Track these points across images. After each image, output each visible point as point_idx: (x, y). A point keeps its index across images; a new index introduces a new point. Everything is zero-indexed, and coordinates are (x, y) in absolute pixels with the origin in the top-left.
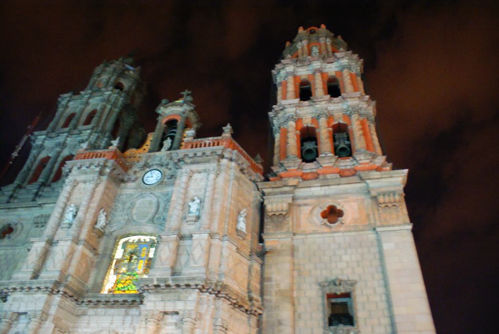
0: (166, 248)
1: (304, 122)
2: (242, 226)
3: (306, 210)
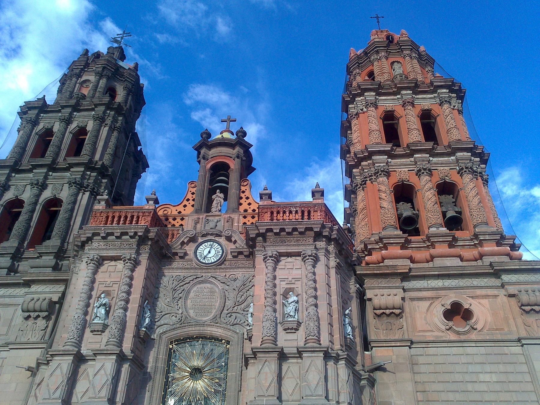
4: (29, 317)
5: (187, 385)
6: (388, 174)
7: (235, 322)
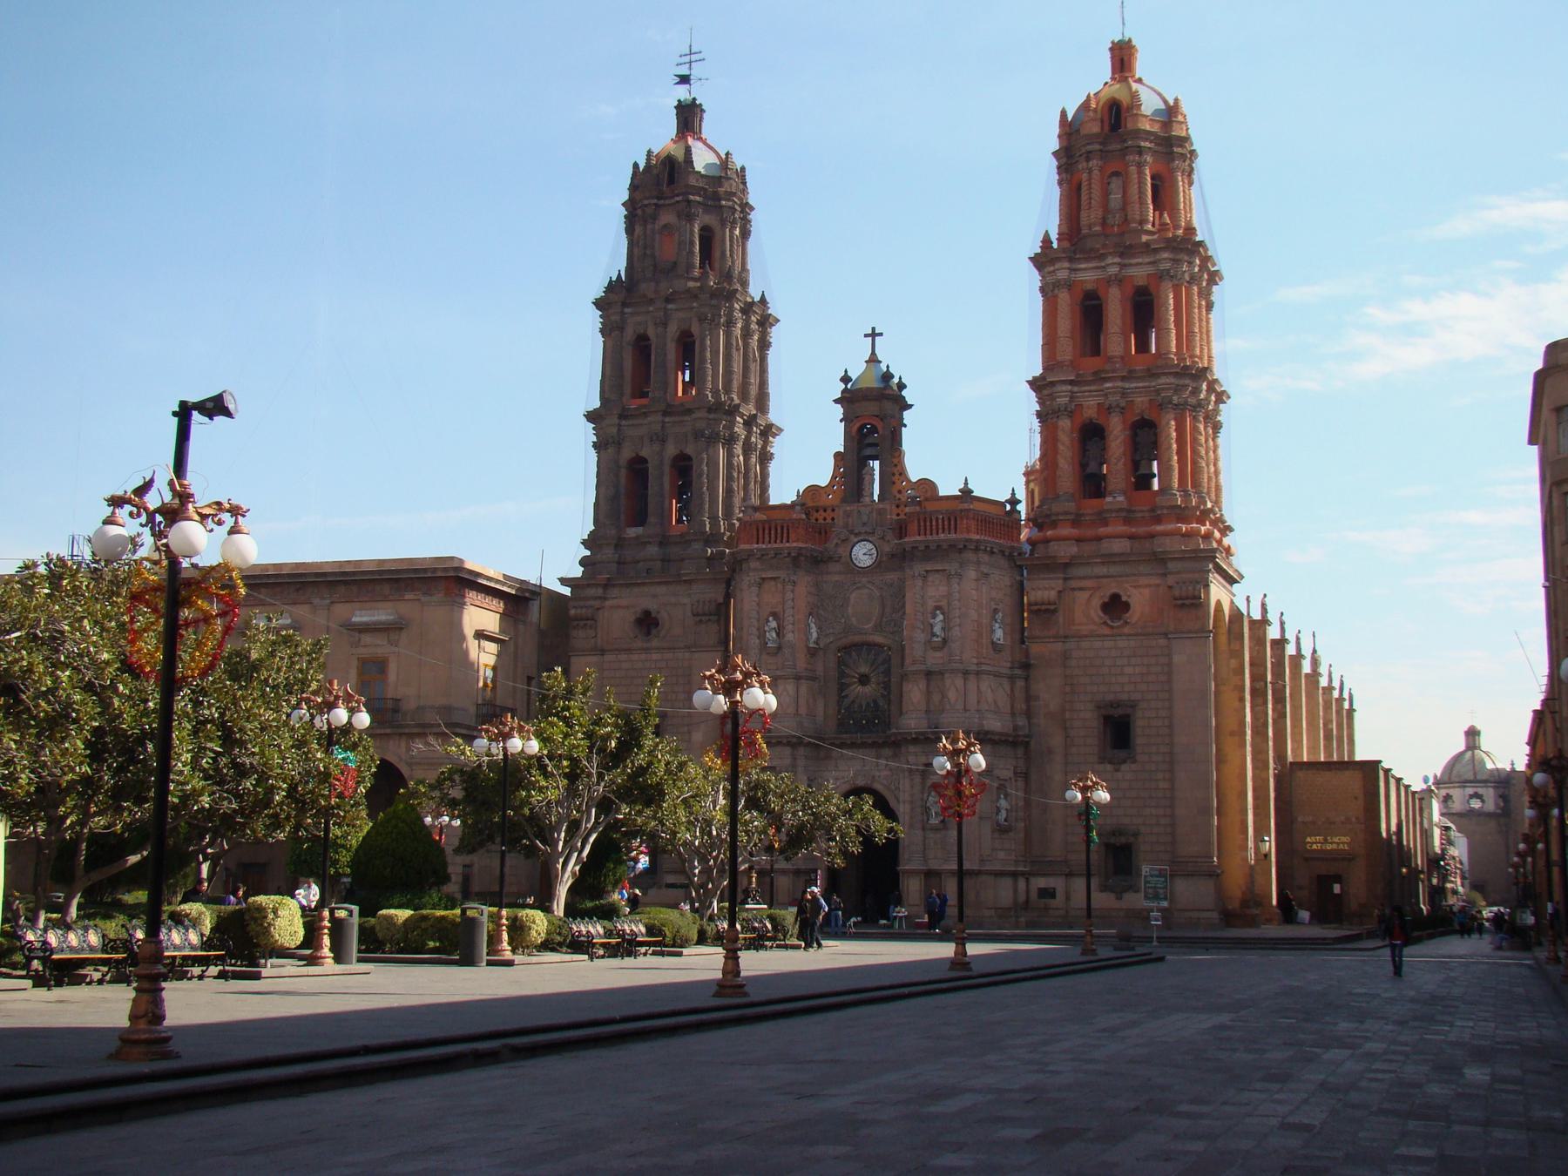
0: (916, 688)
1: (1085, 415)
2: (999, 634)
3: (1082, 596)
4: (701, 621)
5: (857, 690)
6: (1071, 415)
7: (895, 629)
